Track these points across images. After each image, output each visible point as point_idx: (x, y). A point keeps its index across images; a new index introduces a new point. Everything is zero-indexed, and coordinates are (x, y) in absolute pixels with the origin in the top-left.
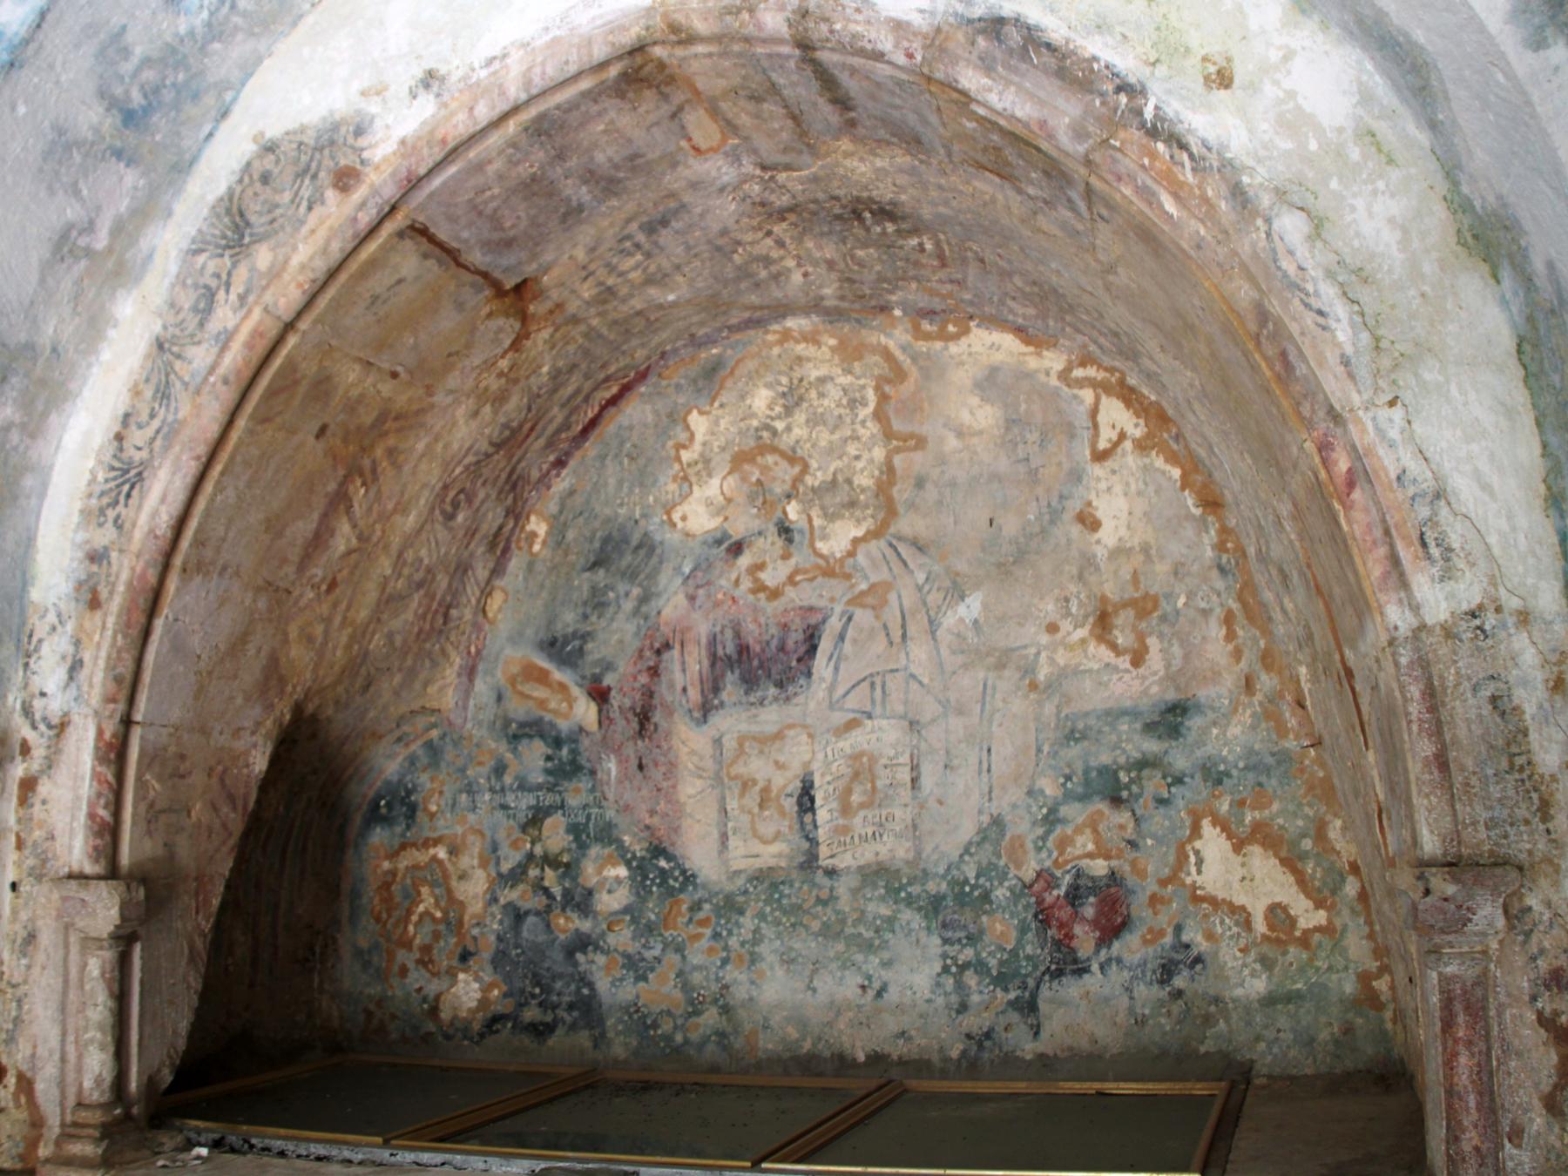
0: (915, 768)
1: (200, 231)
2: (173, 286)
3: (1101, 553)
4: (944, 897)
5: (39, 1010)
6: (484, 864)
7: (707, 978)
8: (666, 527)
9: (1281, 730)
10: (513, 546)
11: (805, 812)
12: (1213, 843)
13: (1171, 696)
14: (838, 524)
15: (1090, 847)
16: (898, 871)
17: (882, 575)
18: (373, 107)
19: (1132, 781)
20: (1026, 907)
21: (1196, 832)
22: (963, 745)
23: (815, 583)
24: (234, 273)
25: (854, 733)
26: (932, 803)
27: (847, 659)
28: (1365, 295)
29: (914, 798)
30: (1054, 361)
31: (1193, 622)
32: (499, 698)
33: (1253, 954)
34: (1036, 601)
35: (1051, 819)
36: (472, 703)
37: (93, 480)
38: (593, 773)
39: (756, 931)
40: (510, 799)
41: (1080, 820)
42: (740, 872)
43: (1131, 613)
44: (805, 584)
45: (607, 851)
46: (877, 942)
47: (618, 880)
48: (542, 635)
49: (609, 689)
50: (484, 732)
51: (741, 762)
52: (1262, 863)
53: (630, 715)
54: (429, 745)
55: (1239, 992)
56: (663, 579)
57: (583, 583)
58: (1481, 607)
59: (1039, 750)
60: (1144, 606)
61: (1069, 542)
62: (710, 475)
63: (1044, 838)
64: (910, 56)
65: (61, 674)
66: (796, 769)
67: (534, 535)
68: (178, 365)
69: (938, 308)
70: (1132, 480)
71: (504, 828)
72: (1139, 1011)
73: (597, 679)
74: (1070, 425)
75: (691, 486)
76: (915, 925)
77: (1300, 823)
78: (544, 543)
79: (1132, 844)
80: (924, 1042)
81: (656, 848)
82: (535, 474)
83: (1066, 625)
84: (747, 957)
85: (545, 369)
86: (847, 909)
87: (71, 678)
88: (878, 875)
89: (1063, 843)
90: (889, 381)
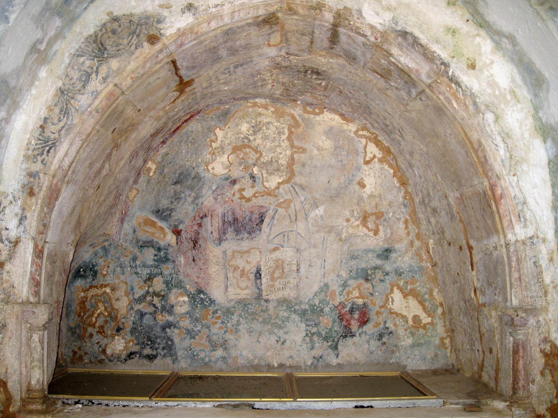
0: (298, 265)
1: (80, 47)
2: (67, 68)
3: (365, 196)
4: (307, 310)
5: (9, 355)
6: (127, 294)
7: (218, 338)
8: (206, 171)
9: (421, 260)
10: (142, 172)
11: (258, 279)
12: (397, 295)
13: (386, 246)
14: (272, 177)
15: (357, 295)
16: (291, 301)
17: (288, 197)
18: (166, 13)
19: (372, 273)
20: (335, 315)
21: (392, 291)
22: (316, 258)
23: (264, 197)
24: (100, 68)
25: (276, 252)
26: (304, 278)
27: (275, 225)
28: (509, 142)
29: (298, 276)
30: (353, 127)
31: (394, 222)
32: (134, 231)
33: (408, 331)
34: (343, 210)
35: (345, 285)
36: (123, 232)
37: (29, 143)
38: (174, 262)
39: (238, 321)
40: (139, 270)
41: (354, 286)
42: (233, 300)
43: (374, 217)
44: (260, 197)
45: (179, 291)
46: (283, 325)
47: (184, 301)
48: (153, 208)
49: (181, 230)
50: (128, 244)
51: (233, 260)
52: (413, 303)
53: (190, 241)
54: (104, 248)
55: (403, 343)
56: (204, 191)
57: (171, 189)
58: (533, 236)
59: (342, 262)
60: (379, 215)
61: (355, 191)
62: (223, 153)
63: (342, 291)
64: (376, 39)
65: (15, 221)
66: (254, 263)
67: (149, 169)
68: (72, 101)
69: (314, 103)
70: (377, 172)
71: (136, 282)
72: (371, 349)
73: (176, 226)
74: (357, 150)
75: (216, 157)
76: (296, 320)
77: (425, 290)
78: (155, 172)
79: (372, 294)
80: (298, 359)
81: (200, 290)
82: (155, 146)
83: (352, 220)
84: (235, 330)
85: (176, 110)
86: (272, 314)
87: (20, 223)
88: (284, 302)
89: (349, 293)
90: (294, 127)
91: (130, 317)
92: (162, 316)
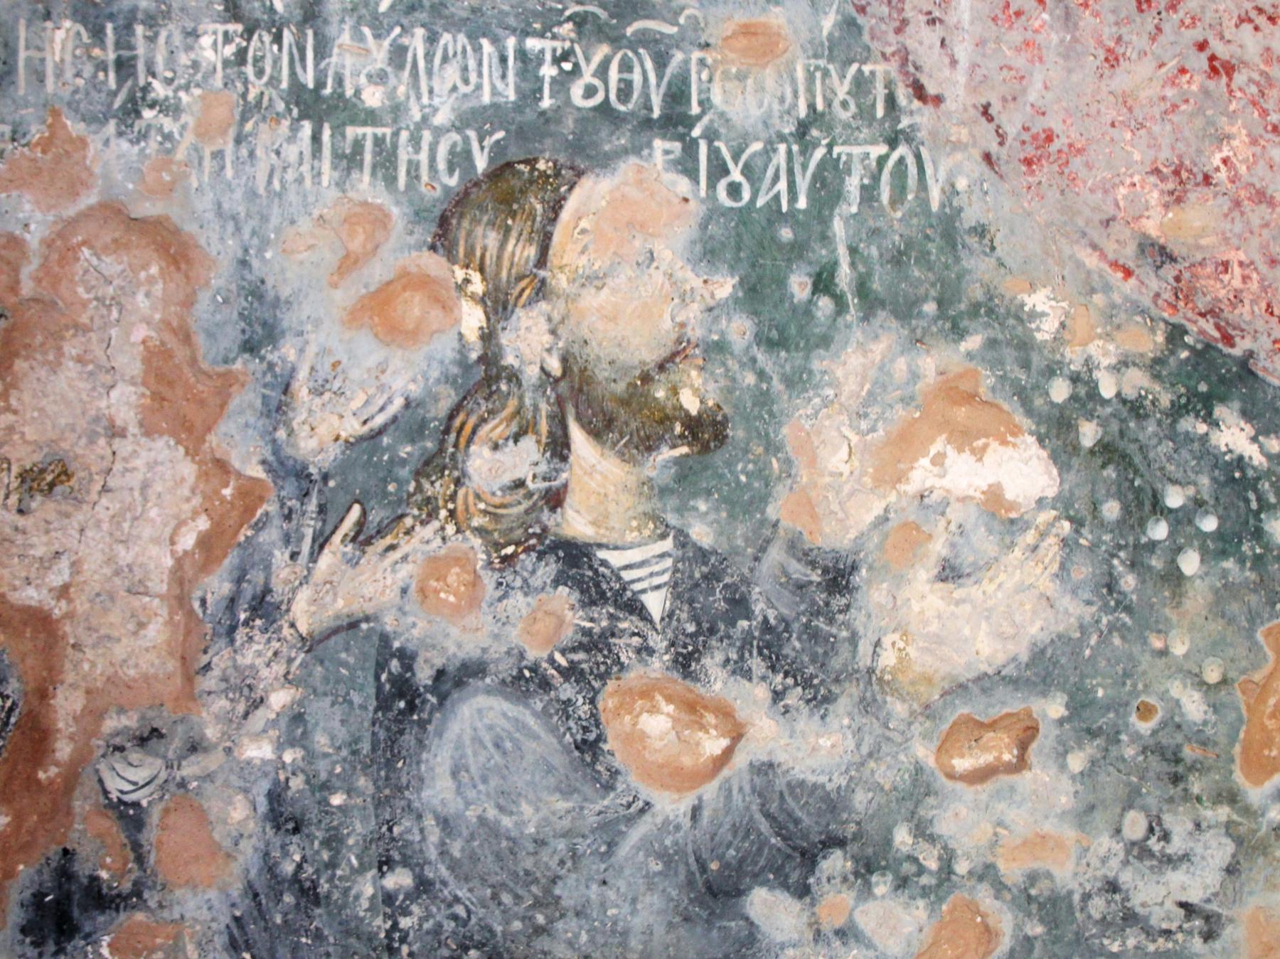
45: (928, 364)
81: (1205, 354)
91: (235, 723)
92: (692, 708)
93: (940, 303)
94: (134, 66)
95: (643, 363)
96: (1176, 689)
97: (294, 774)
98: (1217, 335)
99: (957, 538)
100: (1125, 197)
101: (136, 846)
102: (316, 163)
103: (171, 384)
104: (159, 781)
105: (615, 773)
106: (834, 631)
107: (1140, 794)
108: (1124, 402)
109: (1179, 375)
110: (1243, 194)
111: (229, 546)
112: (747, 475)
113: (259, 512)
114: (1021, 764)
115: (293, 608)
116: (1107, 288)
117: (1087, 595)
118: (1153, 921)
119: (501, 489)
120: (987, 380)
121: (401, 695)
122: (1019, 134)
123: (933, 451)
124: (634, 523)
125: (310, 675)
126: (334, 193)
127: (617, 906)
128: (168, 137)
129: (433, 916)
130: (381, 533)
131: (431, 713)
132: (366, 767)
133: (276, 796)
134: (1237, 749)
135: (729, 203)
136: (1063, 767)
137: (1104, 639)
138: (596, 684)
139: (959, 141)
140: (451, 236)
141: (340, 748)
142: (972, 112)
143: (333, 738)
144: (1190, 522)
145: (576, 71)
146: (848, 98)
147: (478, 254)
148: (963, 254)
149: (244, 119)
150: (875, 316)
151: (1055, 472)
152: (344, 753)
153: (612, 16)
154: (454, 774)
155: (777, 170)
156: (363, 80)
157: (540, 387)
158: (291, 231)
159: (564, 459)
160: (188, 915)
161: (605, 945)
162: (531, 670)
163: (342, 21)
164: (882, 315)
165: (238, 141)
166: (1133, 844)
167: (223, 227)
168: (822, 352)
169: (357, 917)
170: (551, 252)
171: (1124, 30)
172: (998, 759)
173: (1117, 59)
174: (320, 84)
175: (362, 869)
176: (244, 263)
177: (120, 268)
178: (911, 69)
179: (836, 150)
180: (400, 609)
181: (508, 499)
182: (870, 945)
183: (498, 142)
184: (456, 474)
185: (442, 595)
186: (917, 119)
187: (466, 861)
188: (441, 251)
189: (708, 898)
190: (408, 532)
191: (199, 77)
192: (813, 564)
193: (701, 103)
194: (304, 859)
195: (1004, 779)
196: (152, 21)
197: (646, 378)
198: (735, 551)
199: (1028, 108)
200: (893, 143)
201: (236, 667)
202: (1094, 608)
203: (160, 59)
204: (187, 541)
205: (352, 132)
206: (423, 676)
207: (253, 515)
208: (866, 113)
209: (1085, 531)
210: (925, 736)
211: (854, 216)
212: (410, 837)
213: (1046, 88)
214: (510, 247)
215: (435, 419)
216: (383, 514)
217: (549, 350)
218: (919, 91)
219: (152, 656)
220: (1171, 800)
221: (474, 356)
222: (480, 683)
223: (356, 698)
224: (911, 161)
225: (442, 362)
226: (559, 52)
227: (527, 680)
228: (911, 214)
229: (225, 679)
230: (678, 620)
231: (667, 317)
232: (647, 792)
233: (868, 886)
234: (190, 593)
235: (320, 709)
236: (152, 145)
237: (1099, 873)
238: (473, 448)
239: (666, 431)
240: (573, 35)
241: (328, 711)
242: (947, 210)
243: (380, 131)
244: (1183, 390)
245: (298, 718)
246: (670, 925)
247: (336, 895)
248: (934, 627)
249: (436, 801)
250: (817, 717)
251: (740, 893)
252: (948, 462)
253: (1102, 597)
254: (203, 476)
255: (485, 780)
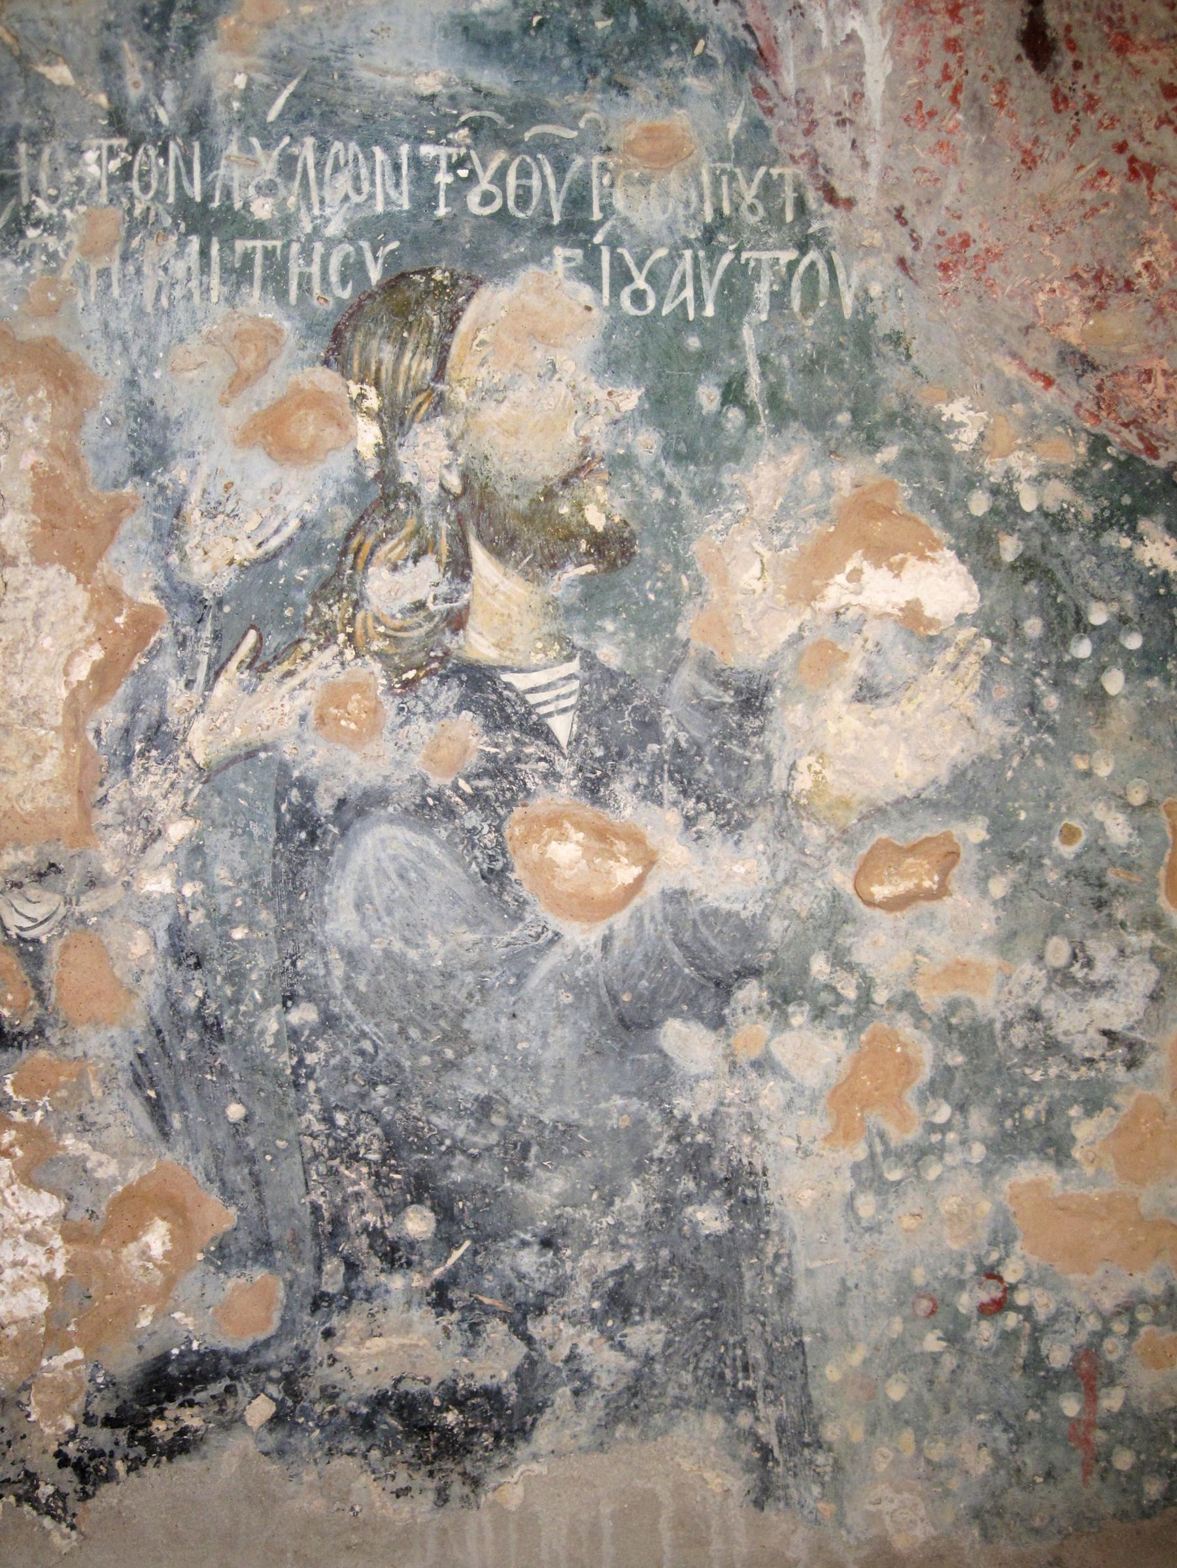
45: (844, 475)
81: (1128, 465)
92: (602, 835)
93: (854, 413)
94: (17, 185)
95: (546, 478)
96: (1100, 812)
97: (194, 908)
98: (1140, 446)
99: (874, 657)
100: (1044, 303)
101: (37, 983)
102: (205, 278)
103: (61, 511)
104: (58, 917)
105: (522, 903)
106: (748, 754)
107: (1063, 920)
108: (1046, 515)
109: (1101, 487)
110: (1165, 300)
111: (123, 675)
112: (656, 593)
113: (153, 639)
114: (942, 892)
115: (189, 738)
116: (1027, 398)
117: (1009, 716)
118: (1076, 1050)
119: (400, 611)
120: (905, 491)
121: (302, 826)
122: (933, 239)
123: (849, 567)
124: (539, 645)
125: (208, 806)
126: (223, 310)
127: (527, 1040)
128: (53, 256)
129: (340, 1052)
130: (277, 659)
131: (333, 843)
132: (267, 900)
133: (176, 931)
134: (1162, 873)
135: (633, 312)
136: (985, 893)
137: (1026, 760)
138: (502, 812)
139: (872, 246)
140: (344, 350)
141: (240, 881)
142: (886, 215)
143: (233, 870)
144: (1114, 639)
145: (473, 178)
146: (756, 201)
147: (373, 368)
148: (877, 362)
149: (130, 236)
150: (787, 427)
151: (975, 587)
152: (245, 885)
153: (509, 121)
154: (358, 906)
155: (683, 277)
156: (252, 191)
157: (440, 505)
158: (180, 350)
159: (465, 579)
160: (91, 1053)
161: (515, 1079)
162: (434, 798)
163: (230, 132)
164: (794, 425)
165: (125, 258)
166: (1056, 971)
167: (111, 347)
168: (732, 465)
169: (262, 1053)
170: (449, 365)
171: (1041, 131)
172: (918, 886)
173: (1034, 161)
174: (208, 197)
175: (266, 1004)
176: (132, 384)
177: (7, 393)
178: (822, 172)
179: (745, 255)
180: (299, 737)
181: (409, 621)
182: (787, 1077)
183: (392, 252)
184: (354, 596)
185: (343, 723)
186: (829, 223)
187: (372, 995)
188: (335, 366)
189: (620, 1030)
190: (307, 657)
191: (83, 193)
192: (725, 685)
193: (602, 208)
194: (207, 995)
195: (925, 905)
196: (34, 138)
197: (549, 494)
198: (644, 672)
199: (943, 212)
200: (803, 248)
201: (132, 800)
202: (1016, 729)
203: (43, 177)
204: (81, 671)
205: (240, 245)
206: (324, 805)
207: (146, 643)
208: (774, 217)
209: (1006, 649)
210: (842, 862)
211: (764, 324)
212: (315, 972)
213: (962, 191)
214: (406, 360)
215: (332, 540)
216: (280, 639)
217: (448, 467)
218: (830, 195)
219: (48, 791)
220: (1095, 926)
221: (370, 474)
222: (382, 812)
223: (256, 830)
224: (822, 266)
225: (337, 481)
226: (454, 159)
227: (431, 808)
228: (823, 321)
229: (122, 812)
230: (586, 744)
231: (570, 431)
232: (555, 923)
233: (785, 1017)
234: (84, 723)
235: (219, 841)
236: (37, 265)
237: (1020, 1001)
238: (371, 570)
239: (570, 548)
240: (468, 141)
241: (228, 843)
242: (861, 317)
243: (270, 244)
244: (1106, 503)
245: (197, 851)
246: (583, 1059)
247: (240, 1031)
248: (851, 749)
249: (340, 935)
250: (730, 843)
251: (653, 1025)
252: (864, 578)
253: (1024, 717)
254: (96, 604)
255: (390, 913)
